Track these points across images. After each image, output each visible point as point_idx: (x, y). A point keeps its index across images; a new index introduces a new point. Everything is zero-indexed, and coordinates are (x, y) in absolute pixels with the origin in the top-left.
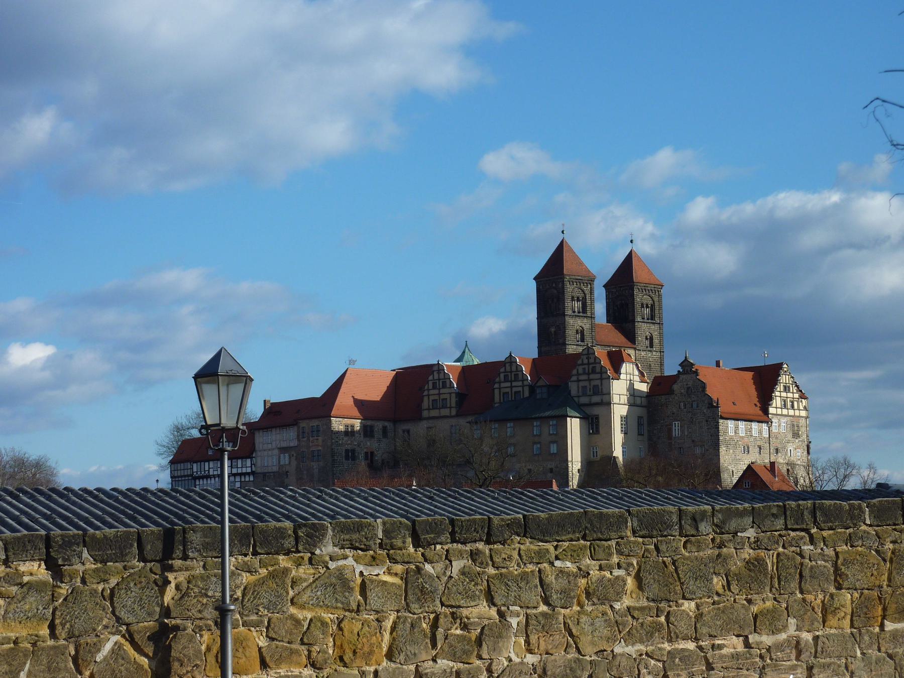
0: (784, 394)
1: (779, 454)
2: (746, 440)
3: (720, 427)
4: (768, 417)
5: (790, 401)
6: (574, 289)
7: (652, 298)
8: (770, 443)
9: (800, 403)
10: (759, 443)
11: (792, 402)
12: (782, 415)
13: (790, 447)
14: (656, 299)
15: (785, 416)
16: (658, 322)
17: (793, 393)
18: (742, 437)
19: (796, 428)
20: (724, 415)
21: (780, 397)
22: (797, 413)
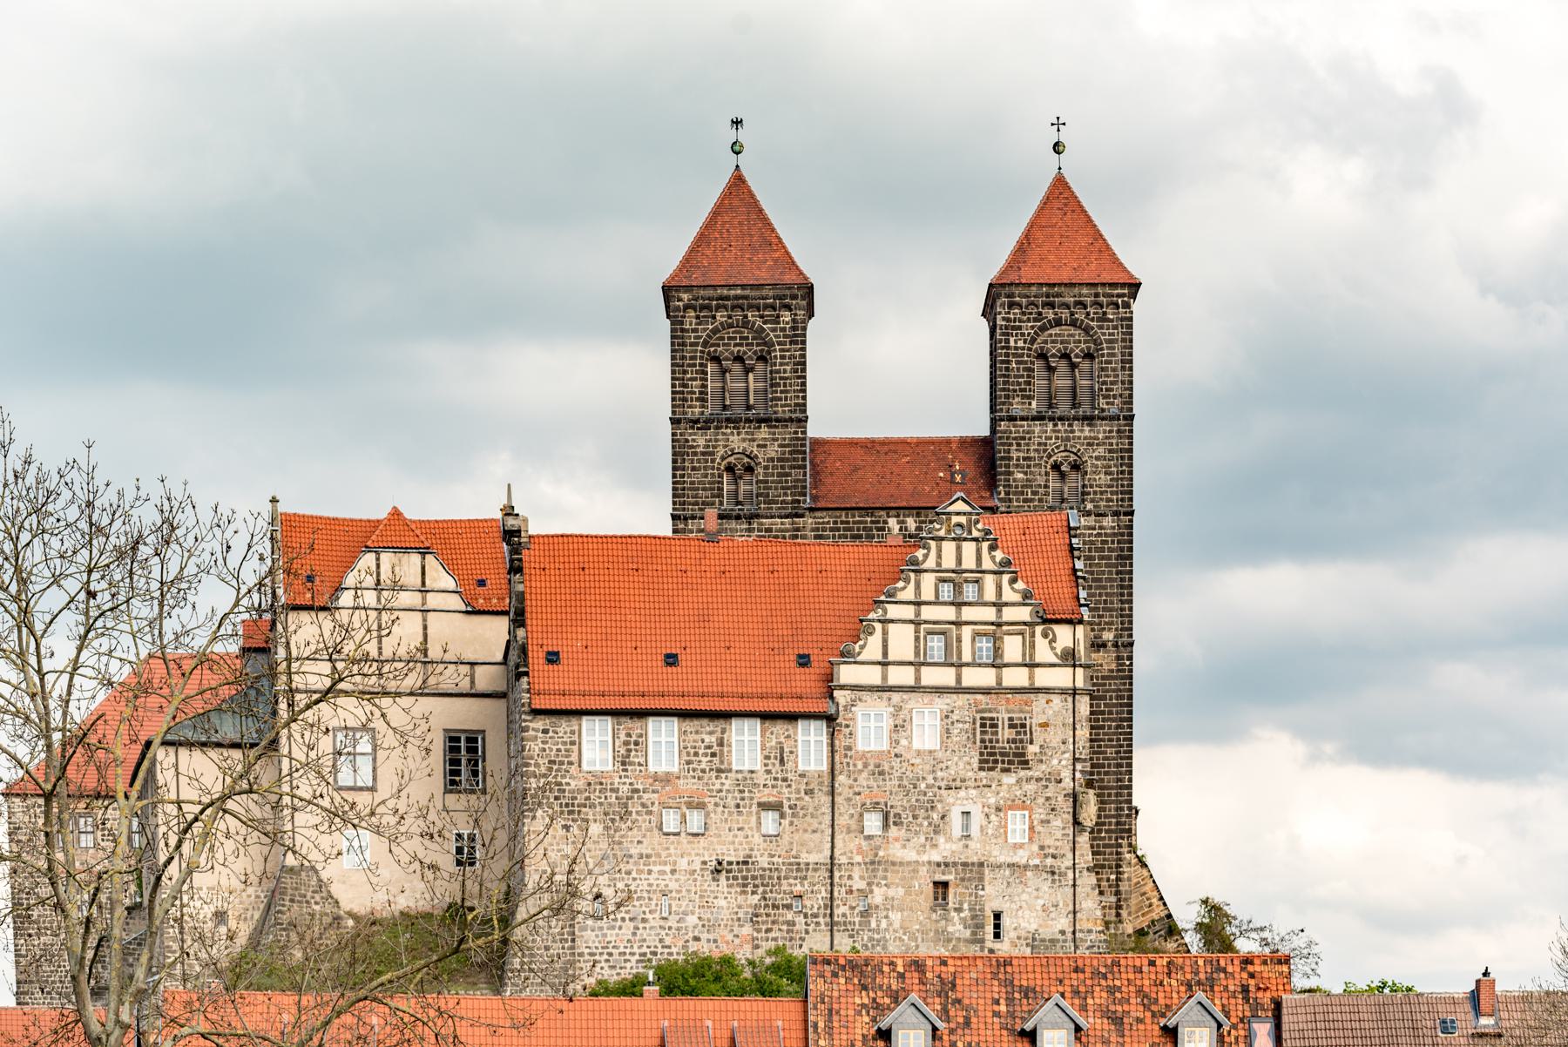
0: (949, 613)
1: (893, 831)
2: (688, 785)
3: (534, 747)
4: (832, 697)
5: (977, 634)
6: (715, 331)
7: (1087, 330)
8: (832, 793)
9: (1041, 644)
10: (767, 796)
11: (997, 640)
12: (916, 689)
13: (956, 803)
14: (1103, 335)
15: (939, 690)
16: (1114, 410)
17: (999, 605)
18: (666, 779)
19: (1005, 733)
20: (539, 703)
21: (916, 623)
22: (1016, 677)
